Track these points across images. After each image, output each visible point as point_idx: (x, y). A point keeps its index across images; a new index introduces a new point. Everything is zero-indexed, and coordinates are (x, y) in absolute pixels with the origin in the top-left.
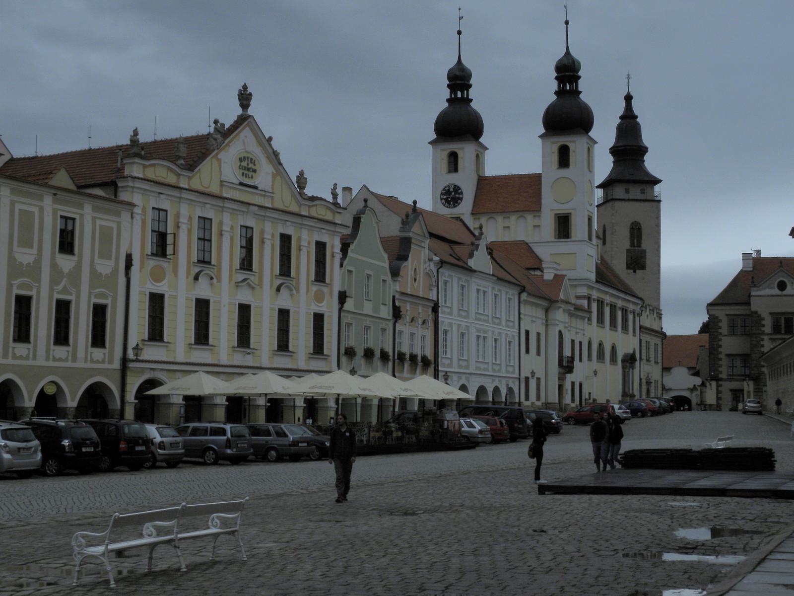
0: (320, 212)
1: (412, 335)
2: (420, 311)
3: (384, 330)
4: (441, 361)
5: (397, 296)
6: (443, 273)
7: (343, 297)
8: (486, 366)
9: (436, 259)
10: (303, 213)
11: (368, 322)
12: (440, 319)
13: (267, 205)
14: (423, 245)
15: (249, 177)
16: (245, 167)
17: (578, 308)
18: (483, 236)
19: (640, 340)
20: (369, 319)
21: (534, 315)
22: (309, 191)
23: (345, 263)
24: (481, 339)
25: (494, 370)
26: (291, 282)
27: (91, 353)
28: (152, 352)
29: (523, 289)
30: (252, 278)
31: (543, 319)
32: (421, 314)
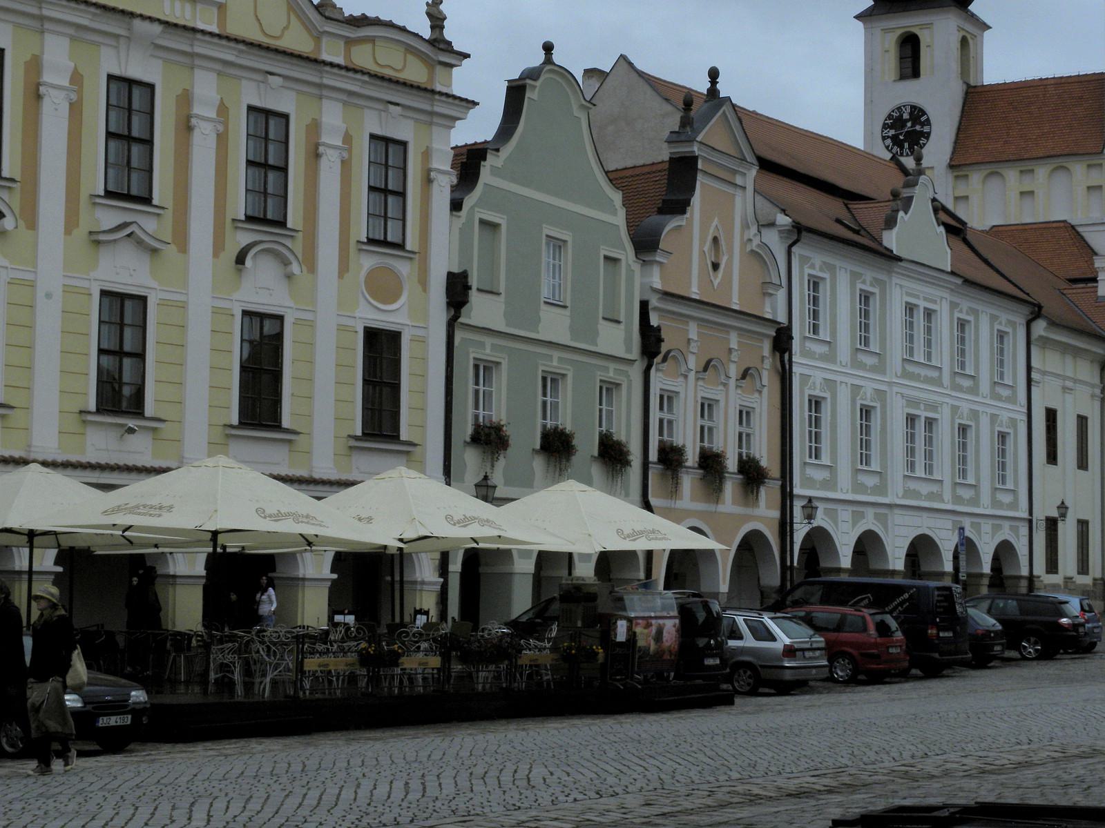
0: (390, 60)
1: (706, 407)
2: (734, 345)
4: (803, 473)
5: (654, 302)
6: (804, 260)
8: (934, 488)
9: (783, 220)
11: (555, 362)
12: (796, 369)
14: (739, 180)
18: (922, 179)
20: (556, 354)
21: (1069, 373)
23: (469, 201)
24: (920, 426)
25: (957, 499)
29: (1036, 312)
31: (1093, 386)
32: (734, 354)
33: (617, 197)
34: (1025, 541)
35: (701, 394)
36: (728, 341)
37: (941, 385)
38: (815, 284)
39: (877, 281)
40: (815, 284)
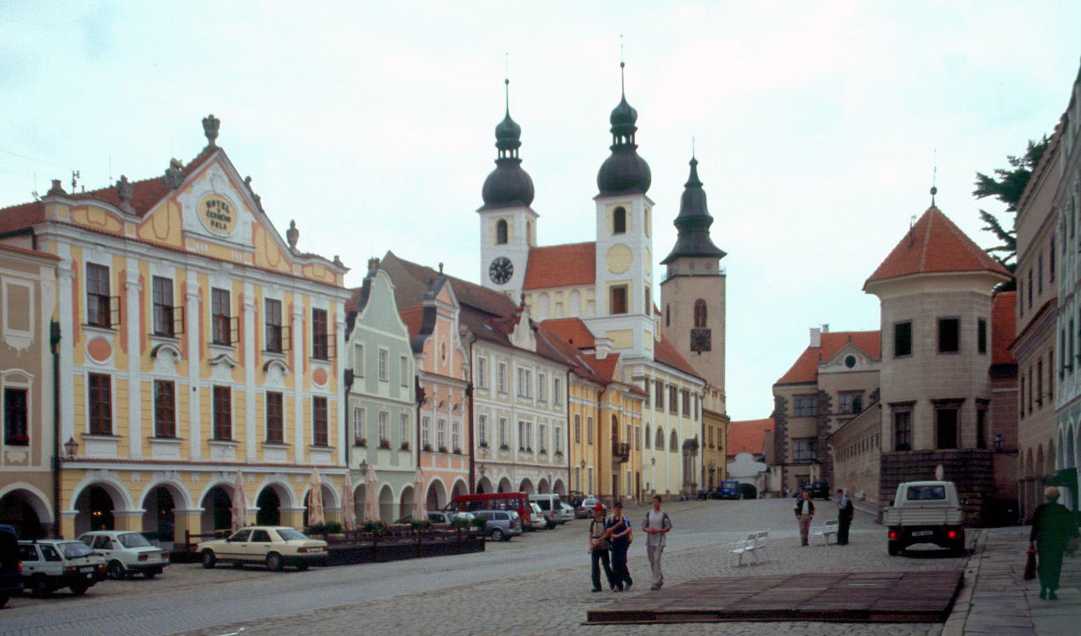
1: (441, 423)
2: (451, 394)
3: (405, 417)
5: (421, 377)
7: (349, 377)
10: (296, 273)
11: (384, 407)
13: (246, 263)
14: (452, 316)
15: (221, 227)
16: (215, 214)
17: (634, 390)
19: (703, 425)
20: (385, 403)
22: (302, 247)
23: (352, 335)
26: (283, 360)
27: (6, 452)
28: (97, 449)
29: (571, 370)
30: (231, 354)
33: (405, 328)
34: (567, 479)
35: (439, 418)
36: (448, 393)
37: (533, 407)
38: (481, 361)
39: (506, 359)
40: (481, 361)
